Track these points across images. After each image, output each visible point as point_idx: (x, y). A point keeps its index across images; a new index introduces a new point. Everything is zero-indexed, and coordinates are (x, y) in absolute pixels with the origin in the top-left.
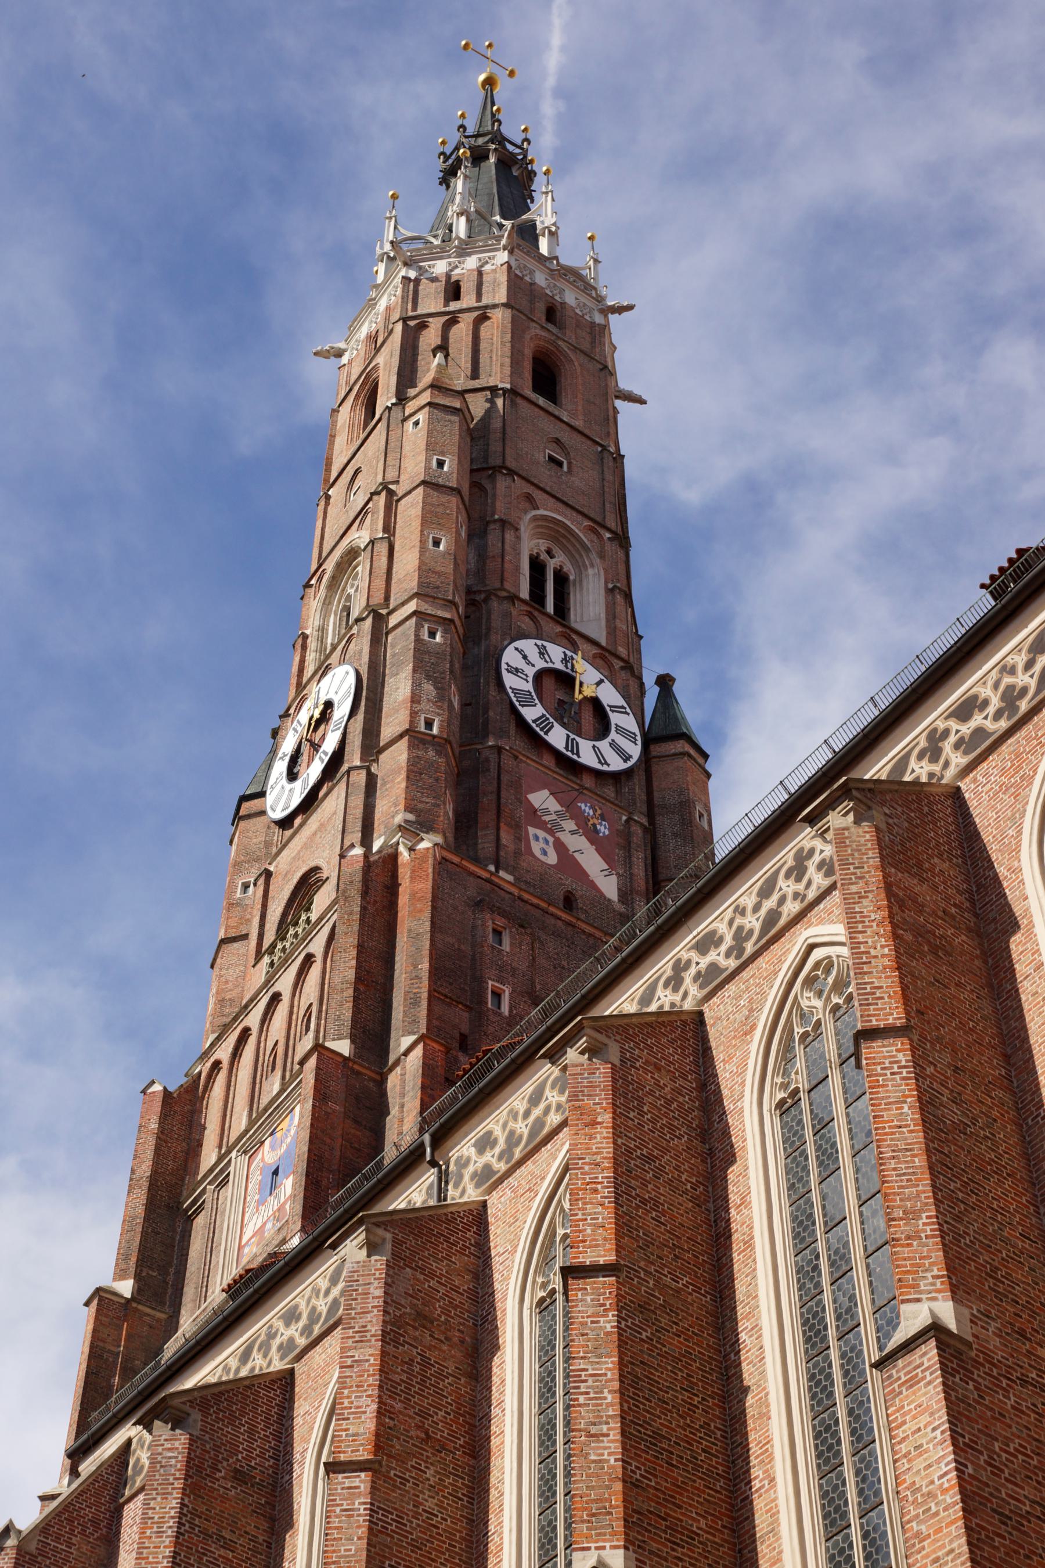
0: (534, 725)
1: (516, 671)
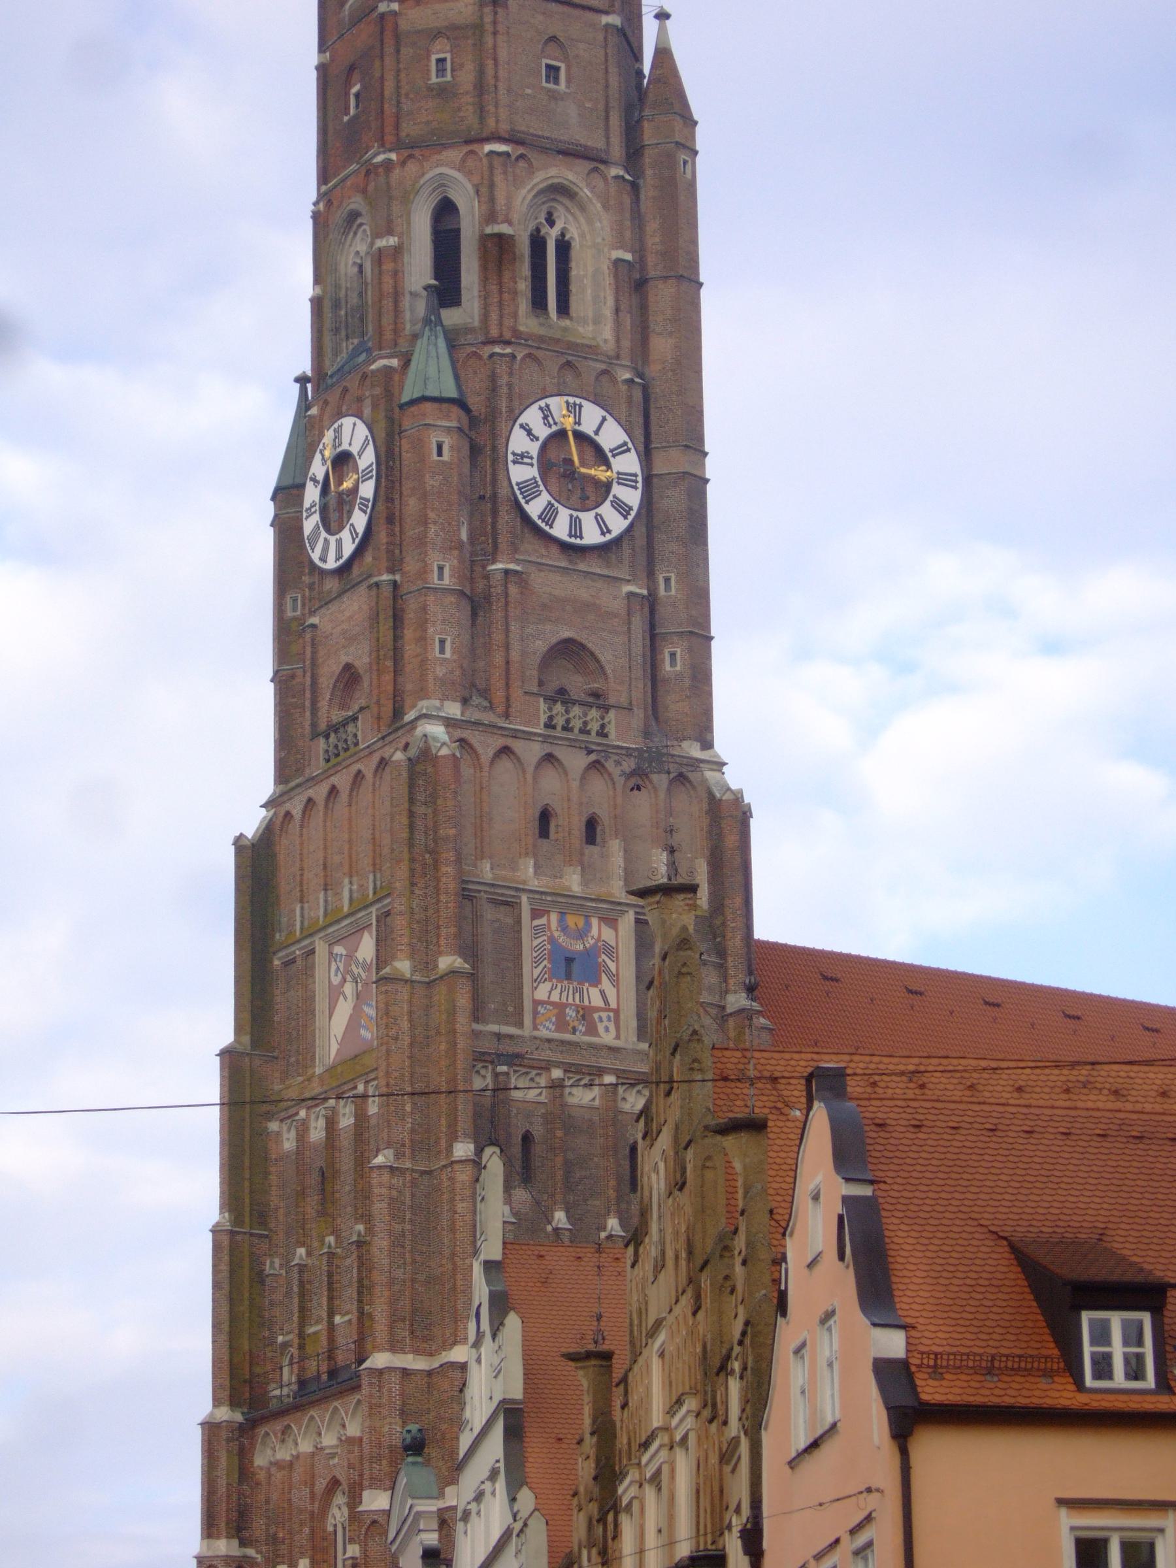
0: (539, 522)
1: (520, 458)
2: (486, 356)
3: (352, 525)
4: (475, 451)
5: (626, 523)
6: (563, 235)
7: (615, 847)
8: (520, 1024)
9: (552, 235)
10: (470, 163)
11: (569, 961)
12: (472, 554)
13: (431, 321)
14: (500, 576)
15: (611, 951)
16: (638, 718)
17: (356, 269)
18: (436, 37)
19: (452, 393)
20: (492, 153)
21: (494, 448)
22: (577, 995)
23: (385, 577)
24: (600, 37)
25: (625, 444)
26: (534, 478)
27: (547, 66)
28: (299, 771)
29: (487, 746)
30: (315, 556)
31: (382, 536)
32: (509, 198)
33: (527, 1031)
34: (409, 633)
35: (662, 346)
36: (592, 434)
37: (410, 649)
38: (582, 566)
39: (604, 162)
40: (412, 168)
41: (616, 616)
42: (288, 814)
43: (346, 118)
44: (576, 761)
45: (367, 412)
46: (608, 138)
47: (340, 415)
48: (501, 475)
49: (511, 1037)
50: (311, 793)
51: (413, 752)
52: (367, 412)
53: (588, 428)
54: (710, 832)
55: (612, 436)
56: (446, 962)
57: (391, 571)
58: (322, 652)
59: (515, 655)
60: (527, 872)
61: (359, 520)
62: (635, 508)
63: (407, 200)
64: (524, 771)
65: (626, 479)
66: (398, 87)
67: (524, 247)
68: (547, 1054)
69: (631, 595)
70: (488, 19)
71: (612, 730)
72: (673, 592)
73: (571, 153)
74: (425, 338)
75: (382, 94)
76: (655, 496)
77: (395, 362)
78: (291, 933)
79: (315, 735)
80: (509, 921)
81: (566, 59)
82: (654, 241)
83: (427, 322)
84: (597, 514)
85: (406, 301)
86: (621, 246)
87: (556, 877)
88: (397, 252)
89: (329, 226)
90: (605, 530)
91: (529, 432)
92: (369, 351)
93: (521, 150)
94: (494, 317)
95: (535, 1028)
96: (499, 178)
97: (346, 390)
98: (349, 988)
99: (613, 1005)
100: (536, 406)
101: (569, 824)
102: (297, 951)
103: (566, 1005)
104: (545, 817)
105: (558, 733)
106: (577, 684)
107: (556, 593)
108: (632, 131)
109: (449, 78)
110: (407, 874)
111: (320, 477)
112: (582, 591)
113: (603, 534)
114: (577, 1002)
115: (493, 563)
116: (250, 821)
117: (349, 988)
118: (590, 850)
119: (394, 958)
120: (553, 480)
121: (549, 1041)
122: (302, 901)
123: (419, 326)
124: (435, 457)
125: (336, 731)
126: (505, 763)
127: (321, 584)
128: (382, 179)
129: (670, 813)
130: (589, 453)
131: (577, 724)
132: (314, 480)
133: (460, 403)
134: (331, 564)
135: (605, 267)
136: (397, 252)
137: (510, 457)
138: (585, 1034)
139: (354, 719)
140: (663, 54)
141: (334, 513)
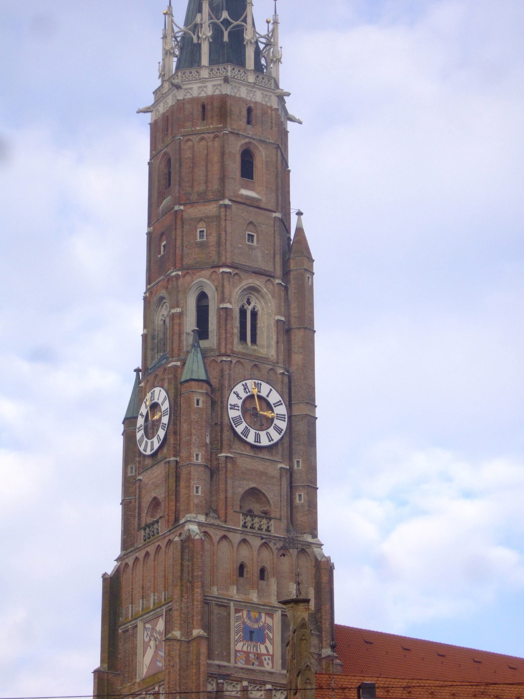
0: (241, 435)
1: (234, 407)
2: (219, 361)
3: (158, 435)
4: (213, 403)
5: (280, 437)
6: (254, 309)
7: (273, 582)
8: (229, 661)
9: (249, 309)
10: (214, 276)
11: (251, 632)
12: (212, 449)
13: (195, 346)
14: (223, 459)
15: (270, 628)
16: (283, 524)
17: (162, 322)
18: (199, 221)
19: (204, 377)
20: (223, 272)
21: (222, 403)
22: (255, 648)
23: (172, 459)
24: (272, 222)
25: (280, 401)
26: (240, 416)
27: (249, 235)
28: (132, 545)
29: (216, 535)
30: (141, 449)
31: (171, 440)
32: (231, 293)
33: (232, 664)
34: (182, 484)
35: (297, 358)
36: (266, 397)
37: (183, 491)
38: (260, 455)
39: (273, 277)
40: (188, 278)
41: (274, 477)
42: (127, 565)
43: (159, 256)
44: (256, 542)
45: (166, 385)
46: (274, 265)
47: (154, 386)
48: (225, 414)
49: (225, 667)
50: (137, 555)
51: (183, 537)
52: (166, 385)
53: (264, 394)
54: (315, 575)
55: (274, 397)
56: (197, 632)
57: (175, 456)
58: (144, 492)
59: (229, 494)
60: (233, 592)
61: (161, 433)
62: (284, 430)
63: (185, 292)
64: (233, 547)
65: (280, 417)
66: (182, 243)
67: (237, 314)
68: (241, 675)
69: (281, 468)
70: (223, 214)
71: (272, 528)
72: (301, 468)
73: (258, 273)
74: (192, 353)
75: (175, 246)
76: (293, 425)
77: (179, 363)
78: (127, 618)
79: (139, 529)
80: (225, 614)
81: (257, 232)
82: (294, 311)
83: (193, 346)
84: (267, 432)
85: (184, 337)
86: (280, 314)
87: (246, 594)
88: (181, 315)
89: (150, 304)
90: (270, 439)
91: (238, 395)
92: (167, 358)
93: (236, 271)
94: (223, 344)
95: (236, 663)
96: (226, 283)
97: (157, 375)
98: (152, 643)
99: (271, 653)
100: (241, 384)
101: (252, 571)
102: (129, 626)
103: (250, 653)
104: (242, 567)
105: (248, 529)
106: (257, 508)
107: (248, 467)
108: (285, 263)
109: (205, 239)
110: (180, 592)
111: (144, 414)
112: (259, 466)
113: (270, 441)
115: (221, 453)
116: (110, 567)
117: (152, 643)
118: (263, 583)
119: (173, 630)
120: (248, 417)
121: (242, 669)
122: (132, 603)
123: (189, 348)
124: (196, 406)
125: (149, 527)
126: (224, 543)
127: (144, 461)
128: (175, 283)
129: (298, 566)
130: (264, 405)
131: (257, 526)
132: (142, 415)
133: (207, 382)
134: (149, 452)
135: (272, 323)
136: (181, 315)
137: (229, 406)
138: (258, 666)
139: (157, 522)
140: (300, 230)
141: (150, 430)
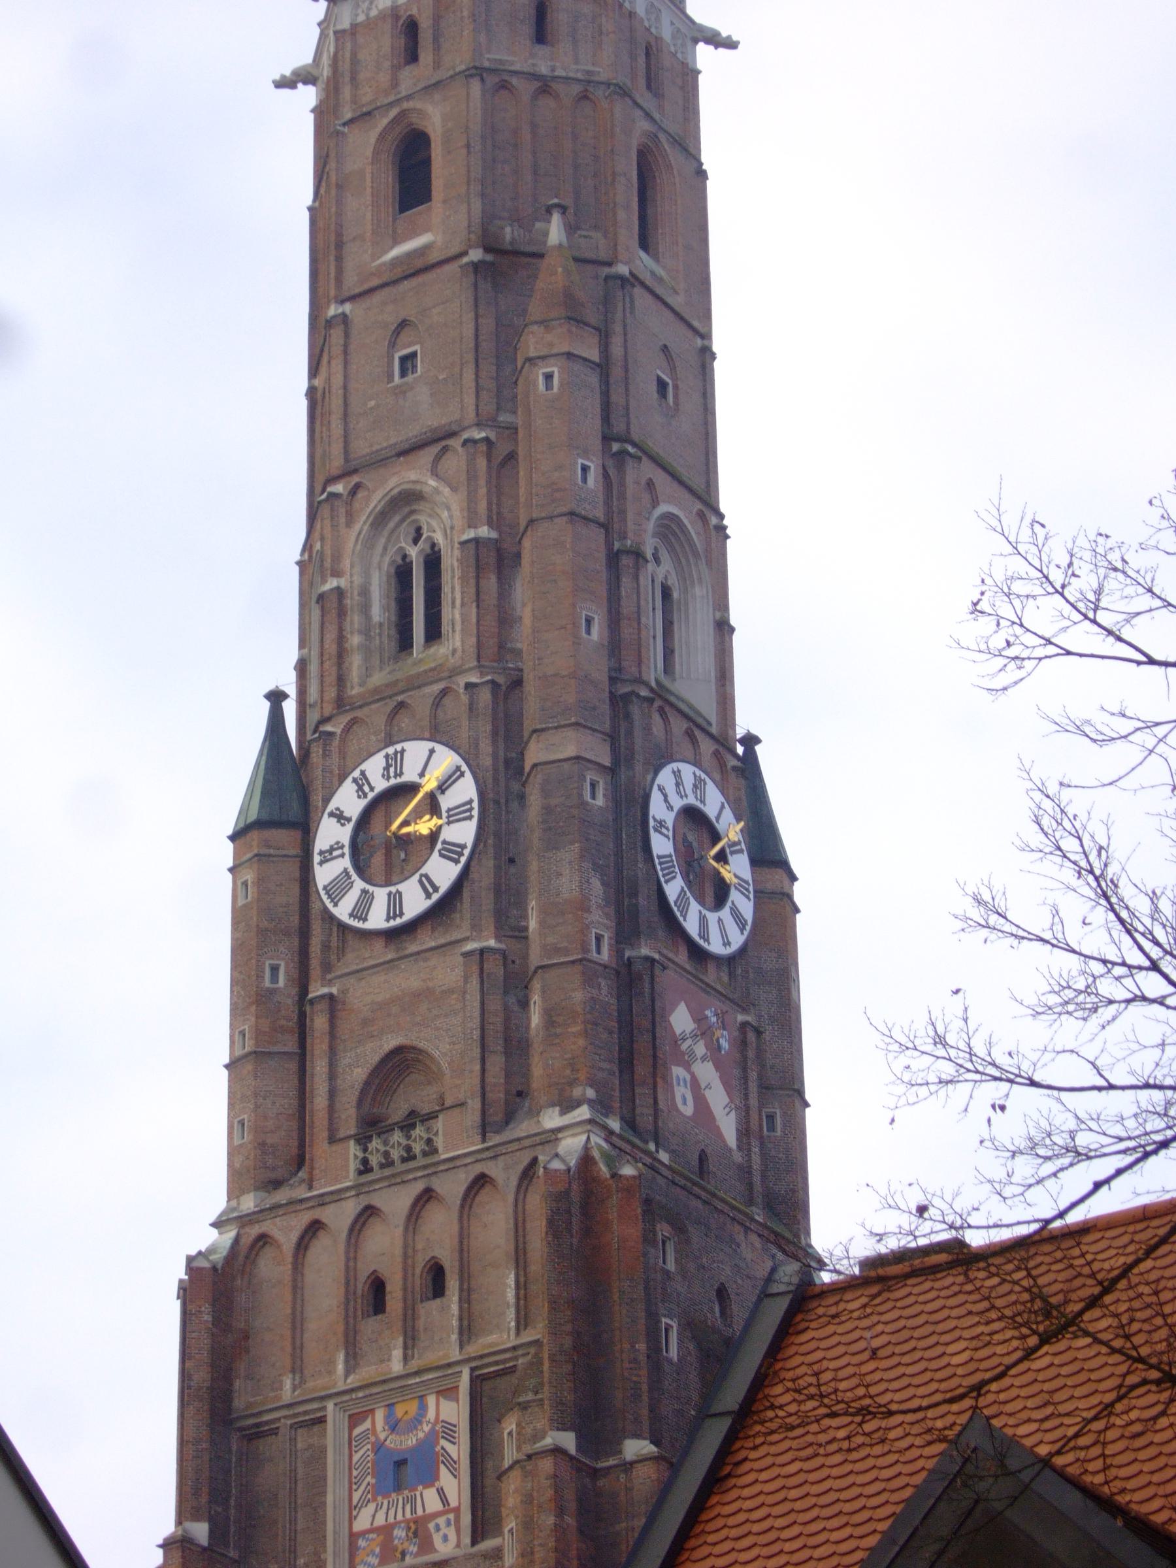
11: (400, 1464)
22: (408, 1507)
38: (413, 948)
87: (382, 1361)
114: (408, 1515)
138: (417, 1555)
